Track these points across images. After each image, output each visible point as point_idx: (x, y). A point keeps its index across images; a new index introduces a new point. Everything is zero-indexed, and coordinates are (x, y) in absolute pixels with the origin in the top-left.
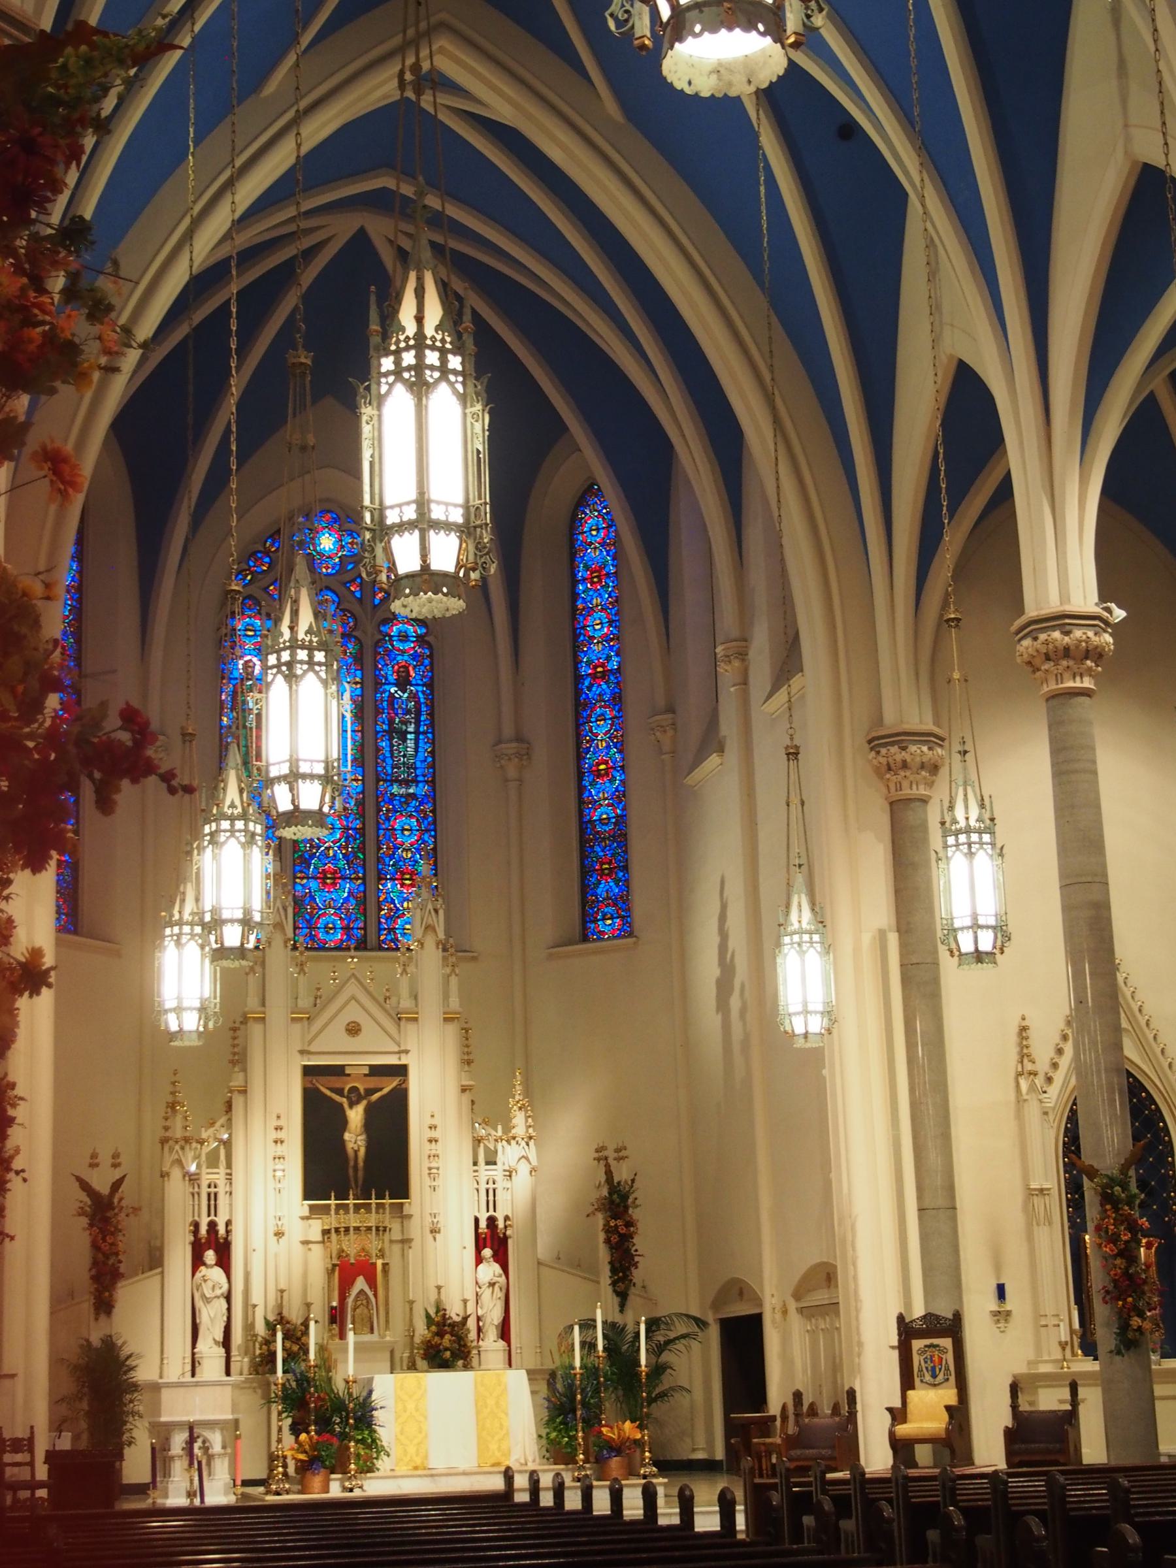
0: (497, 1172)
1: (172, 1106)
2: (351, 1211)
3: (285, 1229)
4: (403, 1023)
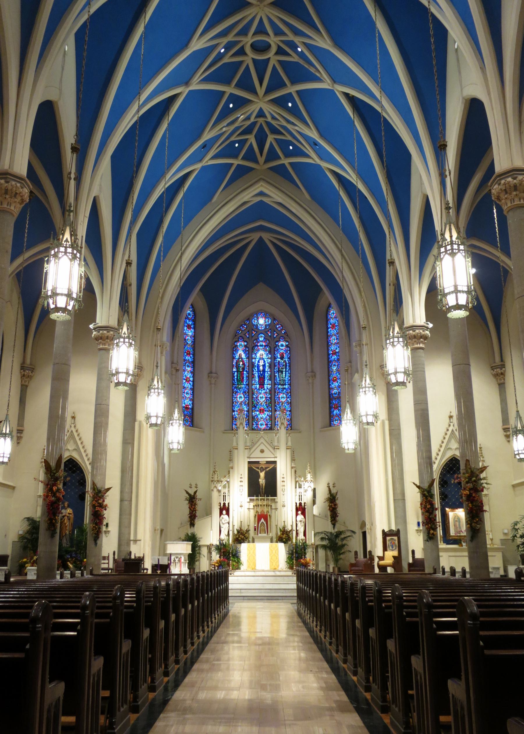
0: (302, 490)
1: (214, 472)
3: (243, 505)
4: (275, 449)
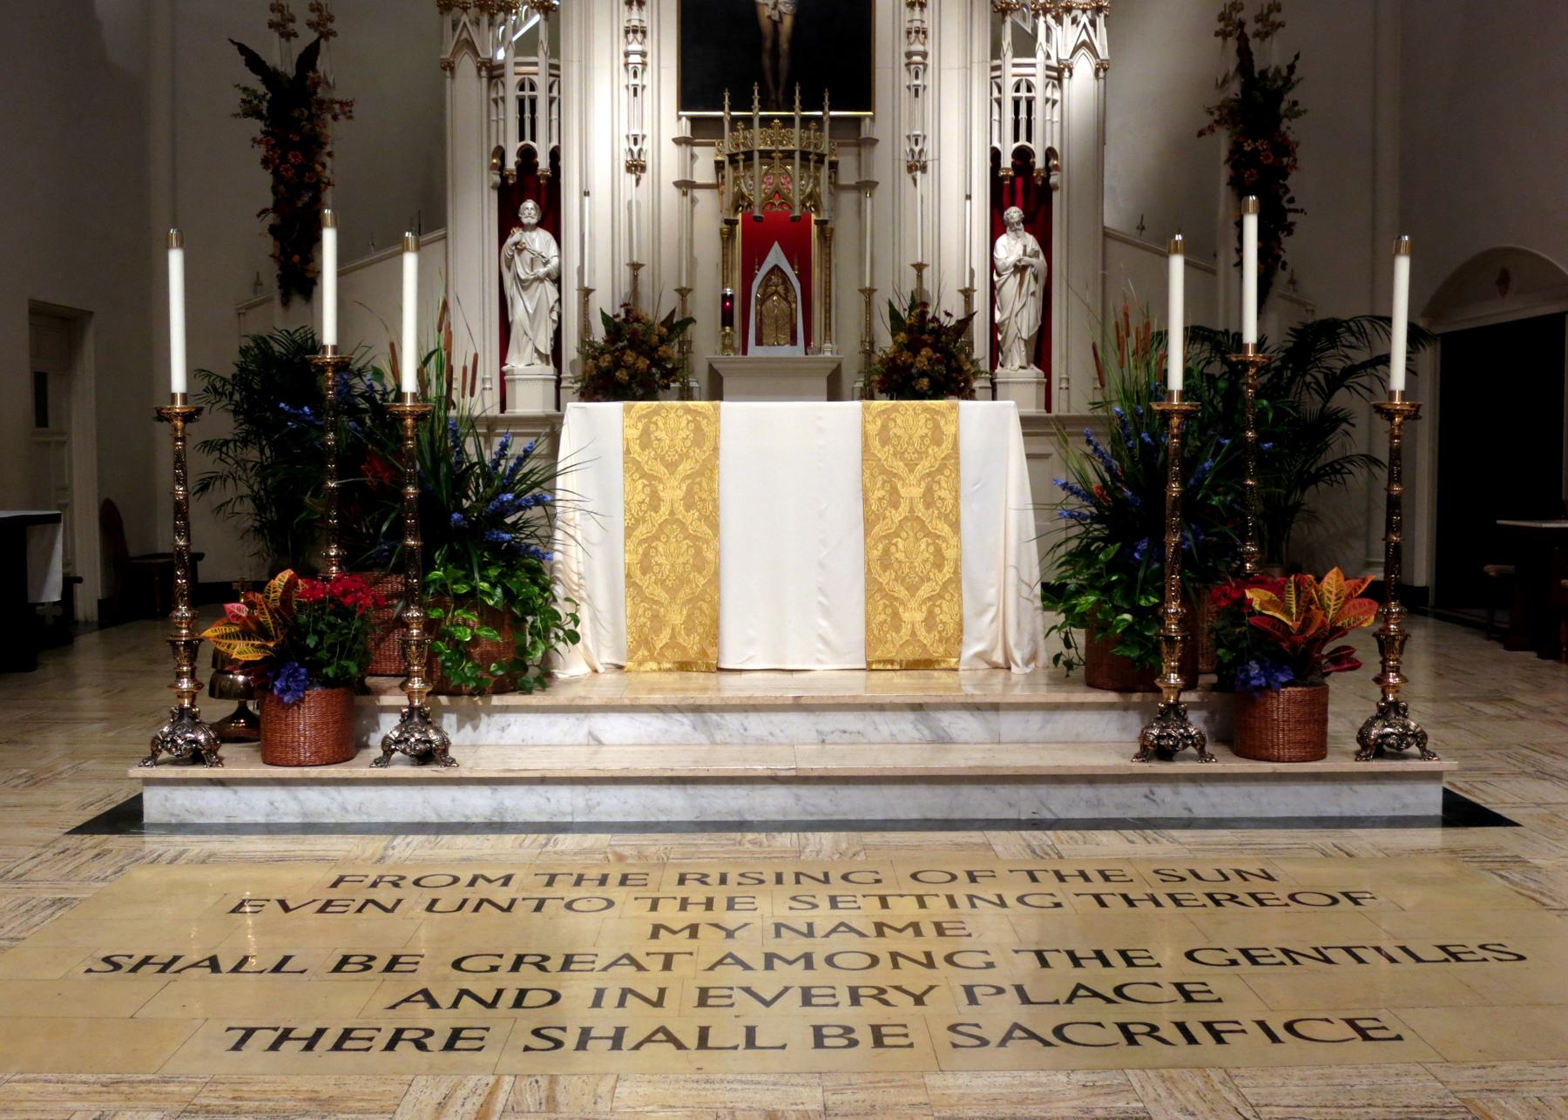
2: (756, 122)
3: (648, 159)
